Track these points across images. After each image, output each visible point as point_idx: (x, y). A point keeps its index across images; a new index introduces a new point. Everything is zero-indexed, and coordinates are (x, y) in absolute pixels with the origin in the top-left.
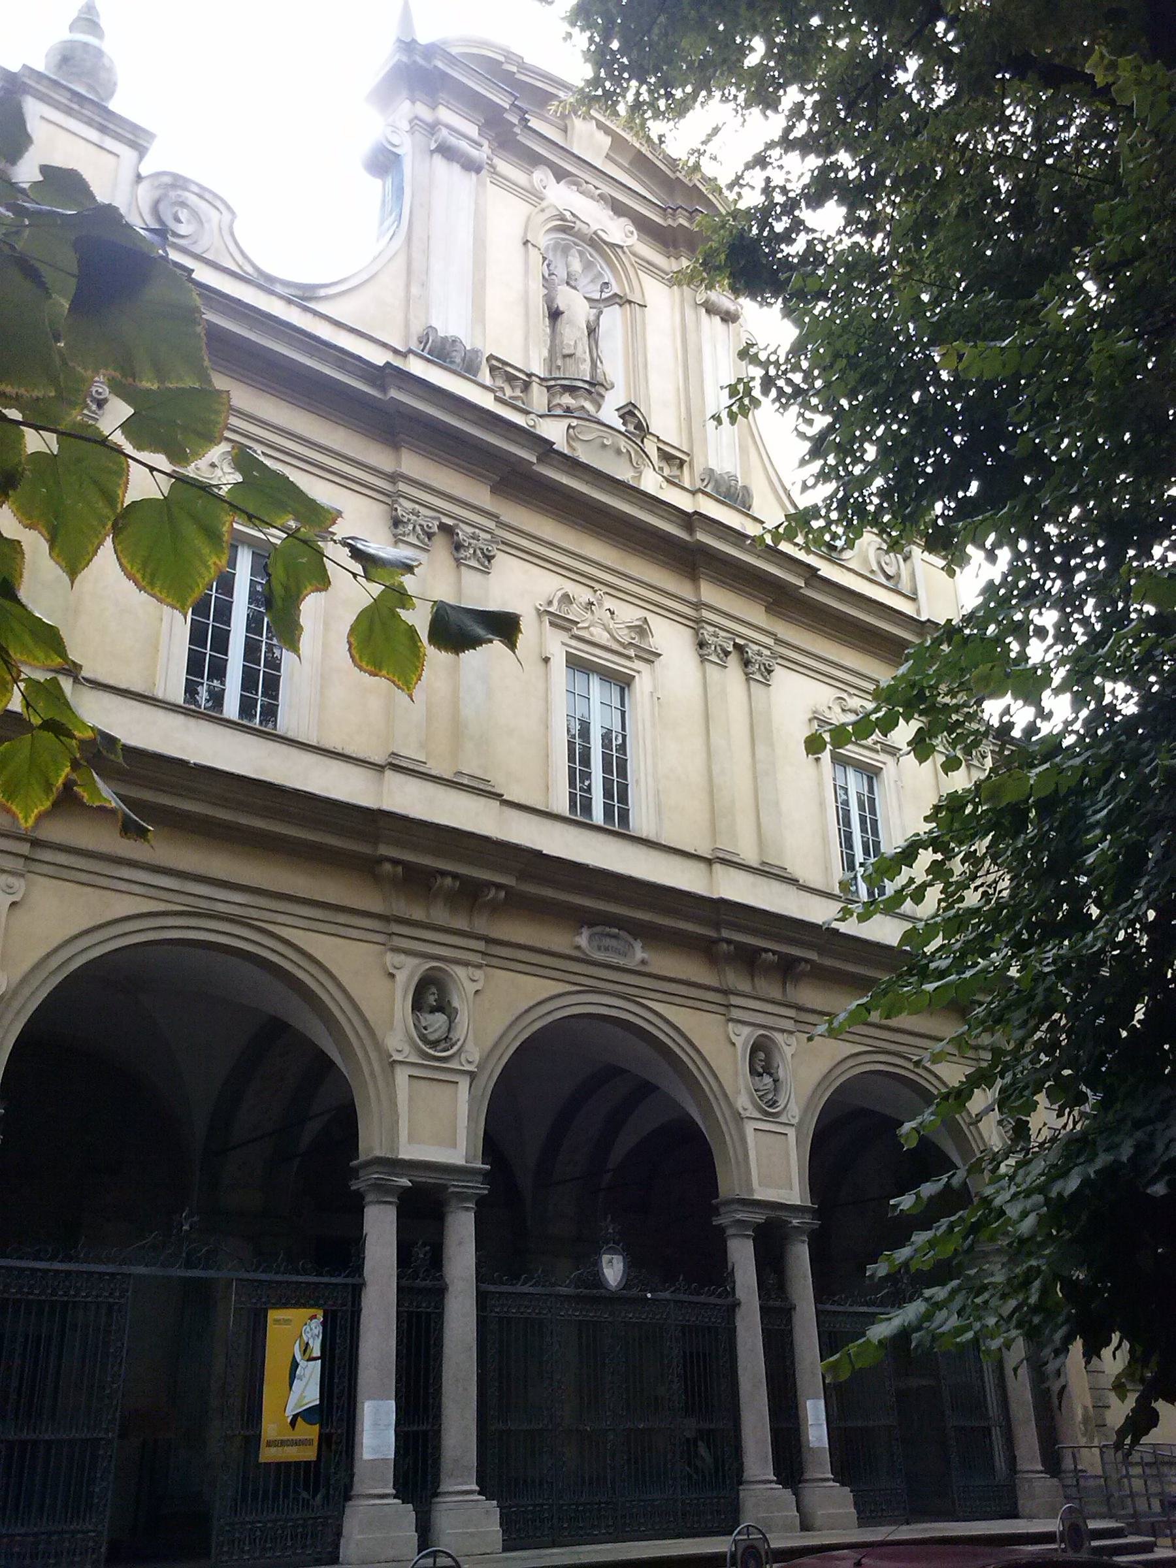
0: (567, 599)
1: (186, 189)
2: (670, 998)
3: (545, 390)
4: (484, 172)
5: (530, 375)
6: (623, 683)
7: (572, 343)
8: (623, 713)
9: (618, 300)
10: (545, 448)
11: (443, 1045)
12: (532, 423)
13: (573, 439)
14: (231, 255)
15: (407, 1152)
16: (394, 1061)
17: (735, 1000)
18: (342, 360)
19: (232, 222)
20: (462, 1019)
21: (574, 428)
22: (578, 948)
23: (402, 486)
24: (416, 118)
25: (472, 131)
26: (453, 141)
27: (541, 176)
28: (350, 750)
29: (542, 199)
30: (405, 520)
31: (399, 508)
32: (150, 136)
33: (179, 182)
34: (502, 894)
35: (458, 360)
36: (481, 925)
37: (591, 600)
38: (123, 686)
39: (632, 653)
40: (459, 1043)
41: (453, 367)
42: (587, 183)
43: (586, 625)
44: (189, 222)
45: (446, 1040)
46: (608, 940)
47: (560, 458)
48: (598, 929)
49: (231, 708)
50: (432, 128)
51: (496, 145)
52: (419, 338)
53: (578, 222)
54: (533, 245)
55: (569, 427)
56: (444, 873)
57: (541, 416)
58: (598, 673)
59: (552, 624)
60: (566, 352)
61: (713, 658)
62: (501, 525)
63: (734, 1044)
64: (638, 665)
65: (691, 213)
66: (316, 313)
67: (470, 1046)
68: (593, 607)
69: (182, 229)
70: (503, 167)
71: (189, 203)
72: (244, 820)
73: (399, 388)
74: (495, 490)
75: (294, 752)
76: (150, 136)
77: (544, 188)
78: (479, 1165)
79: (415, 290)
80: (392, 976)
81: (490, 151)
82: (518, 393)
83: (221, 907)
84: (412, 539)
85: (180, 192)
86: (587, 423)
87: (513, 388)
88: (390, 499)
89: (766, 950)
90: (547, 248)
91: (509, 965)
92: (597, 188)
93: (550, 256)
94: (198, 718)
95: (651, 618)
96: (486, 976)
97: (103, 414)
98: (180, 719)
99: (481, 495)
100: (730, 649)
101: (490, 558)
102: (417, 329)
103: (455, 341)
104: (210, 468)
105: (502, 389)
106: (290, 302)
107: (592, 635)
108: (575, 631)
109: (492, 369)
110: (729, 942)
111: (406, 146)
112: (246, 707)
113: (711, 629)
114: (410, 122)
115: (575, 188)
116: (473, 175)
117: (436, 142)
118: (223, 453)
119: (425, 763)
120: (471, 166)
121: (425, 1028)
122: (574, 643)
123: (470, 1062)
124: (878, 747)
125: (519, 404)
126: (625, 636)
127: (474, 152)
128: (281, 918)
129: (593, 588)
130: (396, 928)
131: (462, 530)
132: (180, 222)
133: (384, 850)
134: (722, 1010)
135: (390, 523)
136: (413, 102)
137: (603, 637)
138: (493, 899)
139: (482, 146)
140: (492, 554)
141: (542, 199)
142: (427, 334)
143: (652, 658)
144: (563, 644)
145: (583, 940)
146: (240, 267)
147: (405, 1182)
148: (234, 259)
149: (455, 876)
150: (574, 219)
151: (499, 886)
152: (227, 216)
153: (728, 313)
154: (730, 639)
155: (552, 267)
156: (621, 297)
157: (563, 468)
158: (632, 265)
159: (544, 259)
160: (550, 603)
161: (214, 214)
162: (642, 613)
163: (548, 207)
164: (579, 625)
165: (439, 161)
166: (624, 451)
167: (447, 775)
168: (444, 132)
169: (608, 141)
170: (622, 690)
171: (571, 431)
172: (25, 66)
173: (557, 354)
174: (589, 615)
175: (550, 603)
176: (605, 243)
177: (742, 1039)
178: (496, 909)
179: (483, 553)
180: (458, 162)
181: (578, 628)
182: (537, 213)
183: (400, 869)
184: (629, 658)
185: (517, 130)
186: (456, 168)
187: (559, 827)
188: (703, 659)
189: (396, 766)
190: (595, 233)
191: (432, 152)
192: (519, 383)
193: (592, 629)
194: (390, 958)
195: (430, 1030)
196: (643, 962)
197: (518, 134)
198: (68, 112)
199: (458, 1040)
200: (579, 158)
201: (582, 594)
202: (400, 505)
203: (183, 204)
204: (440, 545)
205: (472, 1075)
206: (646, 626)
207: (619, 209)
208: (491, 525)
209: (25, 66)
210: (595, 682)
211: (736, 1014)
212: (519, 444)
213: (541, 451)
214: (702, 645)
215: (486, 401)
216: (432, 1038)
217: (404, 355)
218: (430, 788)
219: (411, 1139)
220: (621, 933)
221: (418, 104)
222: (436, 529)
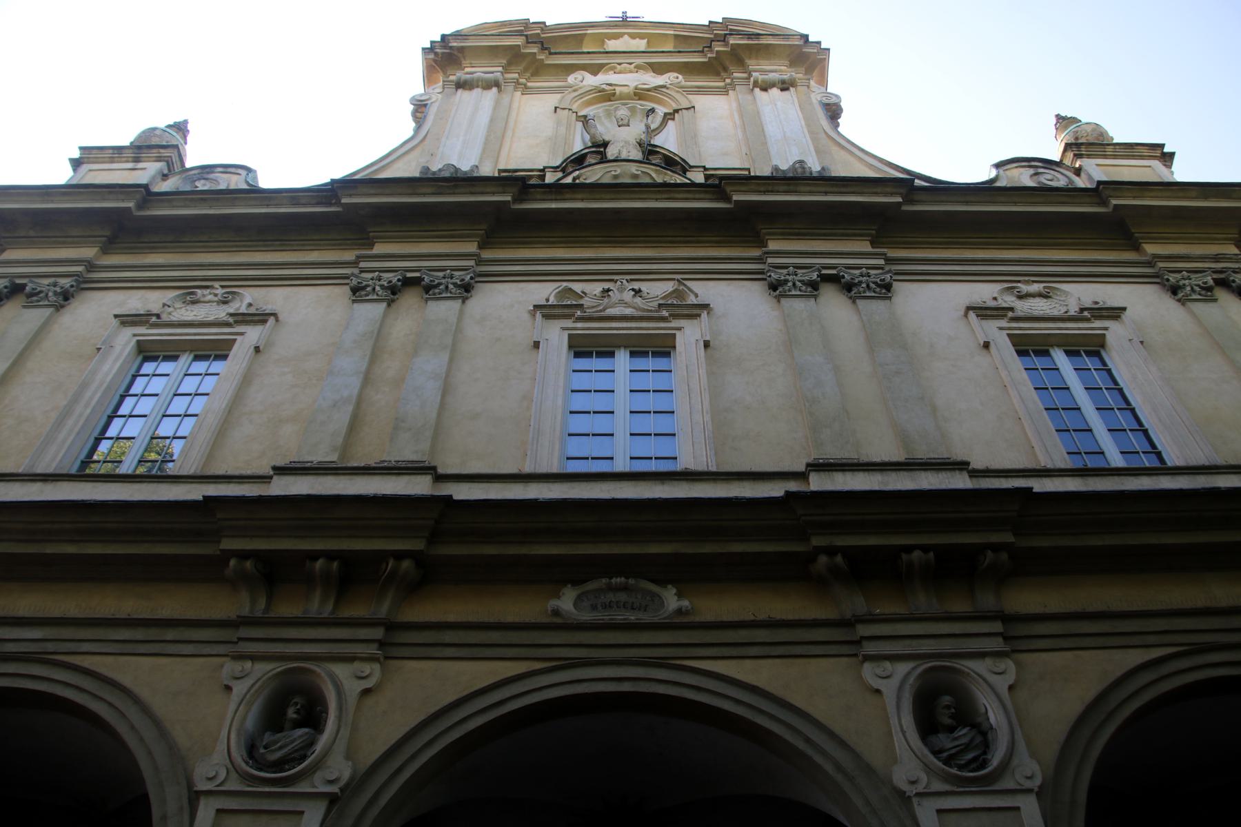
2: (739, 651)
5: (543, 170)
9: (668, 117)
17: (863, 630)
22: (556, 613)
39: (665, 313)
42: (620, 64)
48: (591, 586)
53: (616, 88)
56: (314, 556)
63: (878, 691)
65: (724, 41)
80: (228, 688)
86: (590, 168)
89: (909, 549)
91: (430, 650)
92: (631, 64)
110: (831, 551)
122: (579, 325)
123: (331, 782)
124: (1086, 313)
130: (245, 632)
133: (228, 544)
134: (845, 649)
143: (695, 311)
144: (564, 329)
145: (566, 602)
149: (330, 556)
150: (611, 88)
151: (399, 556)
153: (783, 82)
156: (670, 114)
157: (550, 197)
158: (678, 92)
166: (640, 172)
176: (648, 90)
177: (895, 681)
180: (478, 87)
184: (663, 319)
194: (231, 667)
196: (679, 612)
198: (112, 161)
207: (658, 69)
209: (81, 148)
211: (870, 648)
220: (631, 581)
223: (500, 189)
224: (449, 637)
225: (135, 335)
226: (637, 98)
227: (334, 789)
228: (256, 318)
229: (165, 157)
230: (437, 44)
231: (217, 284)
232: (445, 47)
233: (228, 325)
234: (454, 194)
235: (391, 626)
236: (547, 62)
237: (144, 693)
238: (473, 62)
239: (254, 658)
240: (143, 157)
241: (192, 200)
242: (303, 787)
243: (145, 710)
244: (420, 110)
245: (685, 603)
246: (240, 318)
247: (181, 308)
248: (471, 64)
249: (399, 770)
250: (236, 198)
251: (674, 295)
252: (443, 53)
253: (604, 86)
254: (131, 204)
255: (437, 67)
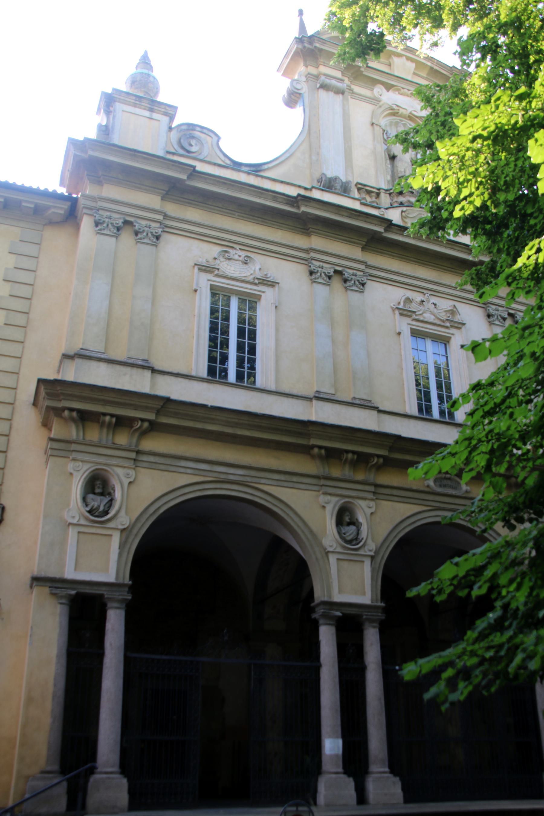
0: (408, 300)
1: (194, 130)
3: (388, 196)
4: (346, 93)
5: (379, 189)
6: (445, 341)
7: (403, 170)
8: (447, 357)
10: (389, 224)
11: (354, 542)
12: (382, 213)
13: (405, 218)
14: (219, 157)
15: (338, 598)
16: (329, 552)
18: (275, 197)
19: (218, 141)
20: (364, 529)
21: (405, 212)
22: (428, 486)
23: (313, 255)
24: (309, 74)
25: (339, 74)
26: (328, 81)
27: (379, 90)
28: (295, 392)
29: (380, 101)
30: (316, 271)
31: (312, 266)
32: (175, 108)
33: (191, 127)
34: (381, 460)
35: (338, 187)
36: (371, 477)
37: (423, 299)
38: (175, 372)
39: (448, 324)
40: (363, 541)
41: (337, 191)
42: (403, 88)
43: (420, 313)
44: (196, 145)
45: (355, 540)
46: (445, 481)
47: (396, 227)
49: (232, 376)
50: (317, 77)
51: (352, 79)
52: (317, 180)
53: (401, 109)
54: (377, 125)
55: (402, 212)
56: (347, 452)
57: (386, 209)
58: (430, 337)
59: (401, 314)
60: (400, 175)
61: (497, 322)
62: (367, 266)
64: (453, 331)
66: (262, 177)
67: (370, 541)
68: (424, 303)
69: (193, 149)
70: (357, 89)
71: (196, 136)
72: (240, 432)
73: (306, 206)
74: (364, 249)
75: (265, 396)
76: (175, 108)
77: (381, 95)
78: (379, 604)
79: (314, 158)
80: (324, 507)
81: (349, 83)
82: (374, 199)
83: (232, 477)
84: (320, 280)
85: (191, 132)
87: (371, 197)
88: (307, 261)
90: (386, 126)
91: (389, 498)
92: (409, 90)
93: (388, 129)
94: (214, 383)
95: (458, 305)
96: (376, 505)
97: (160, 243)
98: (205, 385)
99: (356, 252)
100: (506, 316)
101: (363, 285)
102: (317, 175)
103: (336, 179)
104: (214, 260)
105: (364, 199)
106: (249, 174)
107: (424, 318)
108: (414, 317)
109: (359, 189)
111: (304, 88)
112: (240, 376)
113: (494, 307)
114: (306, 77)
115: (397, 93)
116: (341, 96)
117: (319, 83)
118: (220, 252)
119: (334, 395)
120: (339, 92)
121: (344, 534)
122: (414, 323)
123: (370, 551)
125: (375, 204)
126: (444, 316)
127: (339, 85)
128: (263, 481)
129: (423, 293)
131: (347, 272)
132: (191, 145)
133: (313, 442)
135: (308, 274)
136: (307, 67)
137: (431, 318)
138: (377, 463)
139: (343, 81)
140: (364, 282)
141: (380, 101)
142: (322, 178)
144: (409, 324)
146: (224, 162)
147: (339, 614)
148: (220, 159)
149: (354, 452)
150: (397, 108)
151: (378, 456)
152: (215, 139)
154: (505, 311)
155: (388, 134)
157: (400, 233)
159: (384, 131)
160: (399, 303)
161: (209, 139)
162: (452, 303)
163: (383, 105)
164: (417, 313)
165: (322, 93)
167: (349, 400)
168: (323, 78)
169: (412, 66)
170: (445, 345)
171: (403, 214)
172: (114, 89)
173: (396, 177)
174: (421, 307)
175: (399, 303)
176: (417, 117)
178: (379, 468)
179: (359, 282)
180: (332, 91)
181: (416, 315)
182: (378, 108)
183: (323, 452)
184: (447, 327)
185: (362, 69)
186: (331, 94)
187: (413, 422)
188: (491, 323)
189: (319, 397)
190: (411, 113)
191: (318, 89)
192: (374, 194)
193: (424, 315)
195: (347, 534)
196: (467, 492)
197: (362, 72)
199: (363, 539)
200: (397, 77)
201: (418, 297)
202: (312, 264)
203: (193, 137)
204: (337, 282)
205: (372, 558)
206: (455, 310)
208: (362, 267)
209: (114, 89)
210: (429, 342)
212: (374, 224)
213: (386, 225)
214: (489, 316)
215: (356, 206)
216: (349, 538)
217: (310, 190)
218: (337, 407)
219: (340, 591)
221: (309, 67)
222: (332, 273)
223: (379, 223)
224: (395, 492)
225: (208, 280)
226: (408, 119)
227: (372, 553)
228: (269, 283)
229: (170, 114)
230: (306, 39)
231: (237, 247)
232: (311, 43)
233: (255, 284)
234: (357, 219)
235: (376, 486)
236: (365, 73)
237: (293, 506)
238: (326, 62)
239: (330, 494)
240: (155, 109)
241: (218, 182)
242: (361, 552)
243: (296, 513)
244: (295, 95)
245: (468, 488)
246: (261, 281)
247: (223, 261)
248: (324, 63)
249: (388, 546)
250: (243, 188)
251: (451, 312)
252: (309, 48)
253: (394, 107)
254: (184, 177)
255: (301, 54)
